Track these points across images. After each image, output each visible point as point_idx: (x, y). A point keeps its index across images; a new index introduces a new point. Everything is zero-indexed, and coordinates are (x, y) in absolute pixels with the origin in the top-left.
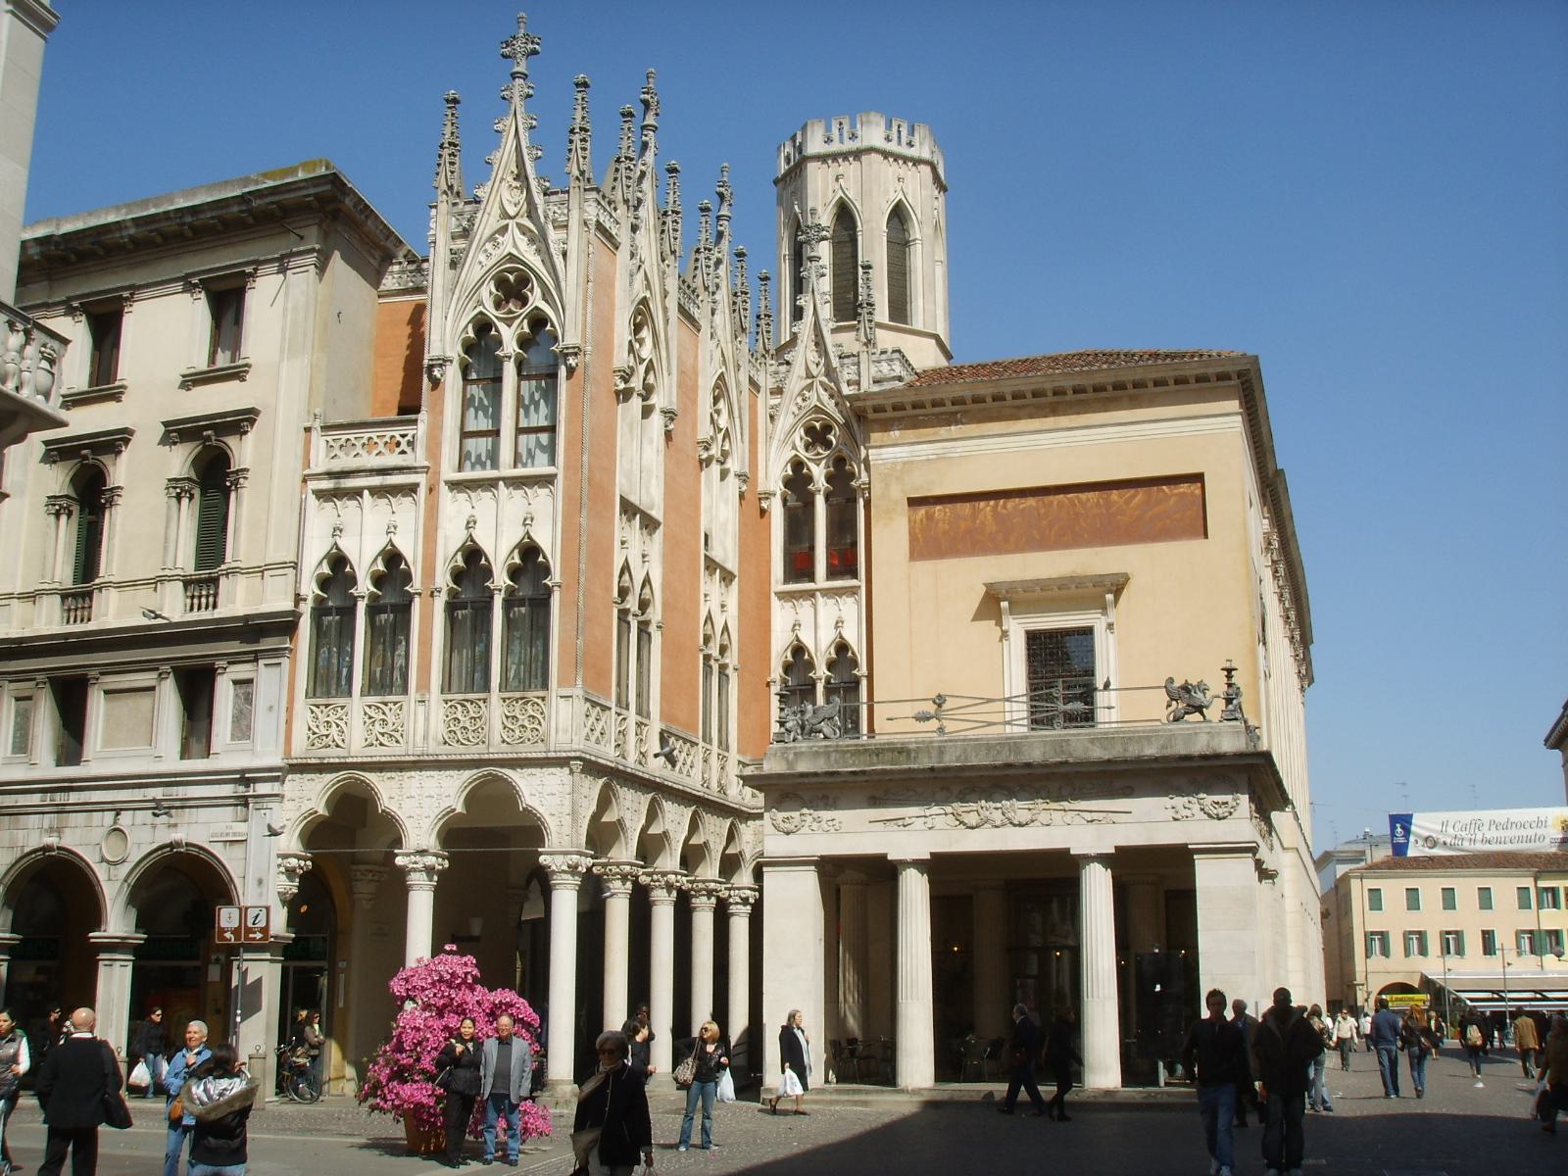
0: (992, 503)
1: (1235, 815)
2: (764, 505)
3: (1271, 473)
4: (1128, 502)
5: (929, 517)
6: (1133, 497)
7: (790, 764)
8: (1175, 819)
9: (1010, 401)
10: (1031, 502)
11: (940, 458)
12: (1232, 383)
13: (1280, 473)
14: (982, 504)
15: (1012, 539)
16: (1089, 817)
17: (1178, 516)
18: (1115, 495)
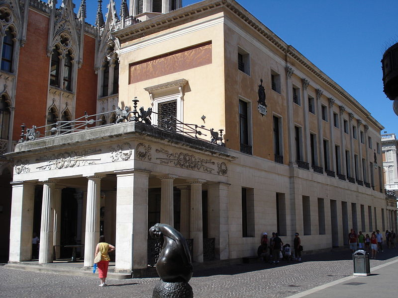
0: (152, 62)
1: (130, 159)
2: (96, 73)
3: (285, 47)
4: (189, 55)
5: (135, 69)
6: (191, 53)
7: (20, 150)
8: (113, 162)
9: (156, 27)
10: (162, 59)
11: (138, 49)
12: (221, 6)
13: (289, 47)
14: (149, 62)
15: (157, 73)
16: (89, 162)
17: (204, 57)
18: (186, 53)
